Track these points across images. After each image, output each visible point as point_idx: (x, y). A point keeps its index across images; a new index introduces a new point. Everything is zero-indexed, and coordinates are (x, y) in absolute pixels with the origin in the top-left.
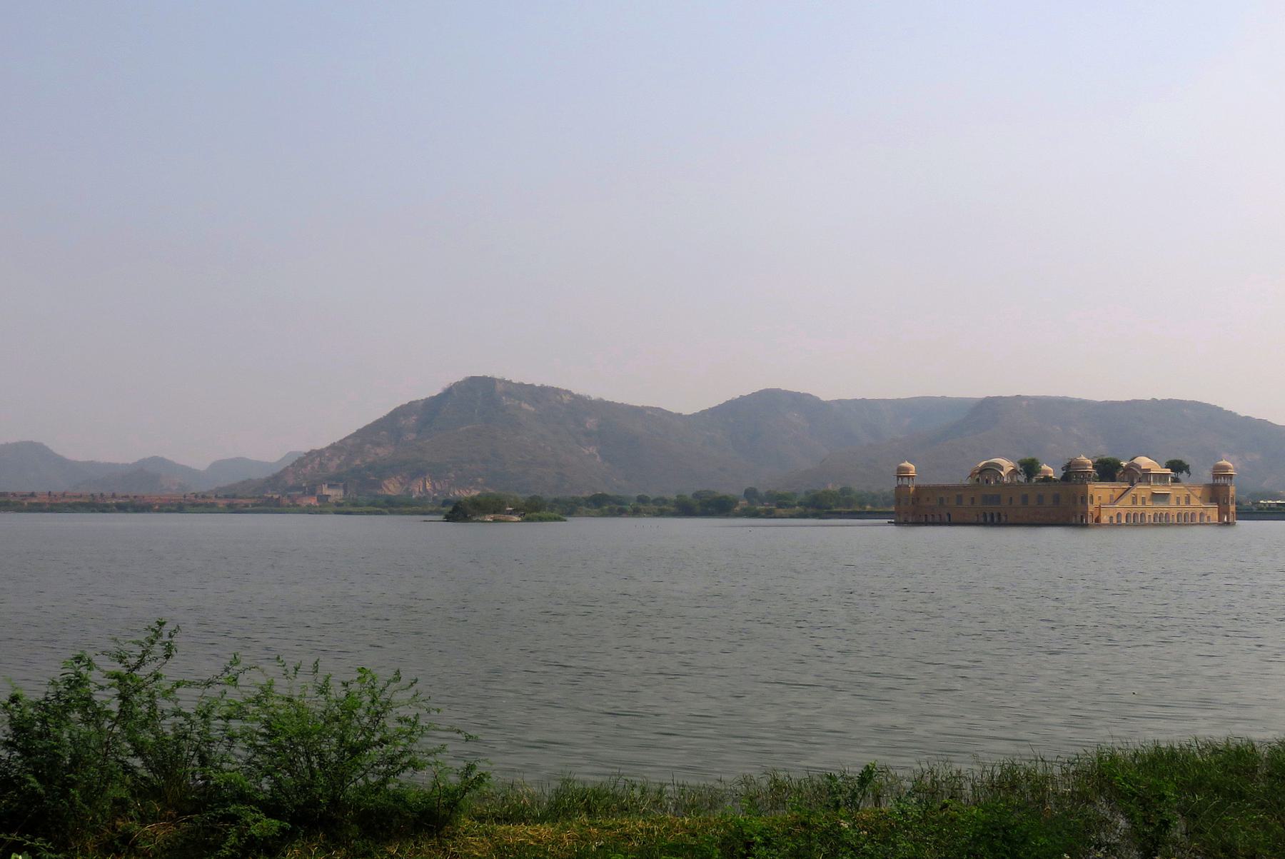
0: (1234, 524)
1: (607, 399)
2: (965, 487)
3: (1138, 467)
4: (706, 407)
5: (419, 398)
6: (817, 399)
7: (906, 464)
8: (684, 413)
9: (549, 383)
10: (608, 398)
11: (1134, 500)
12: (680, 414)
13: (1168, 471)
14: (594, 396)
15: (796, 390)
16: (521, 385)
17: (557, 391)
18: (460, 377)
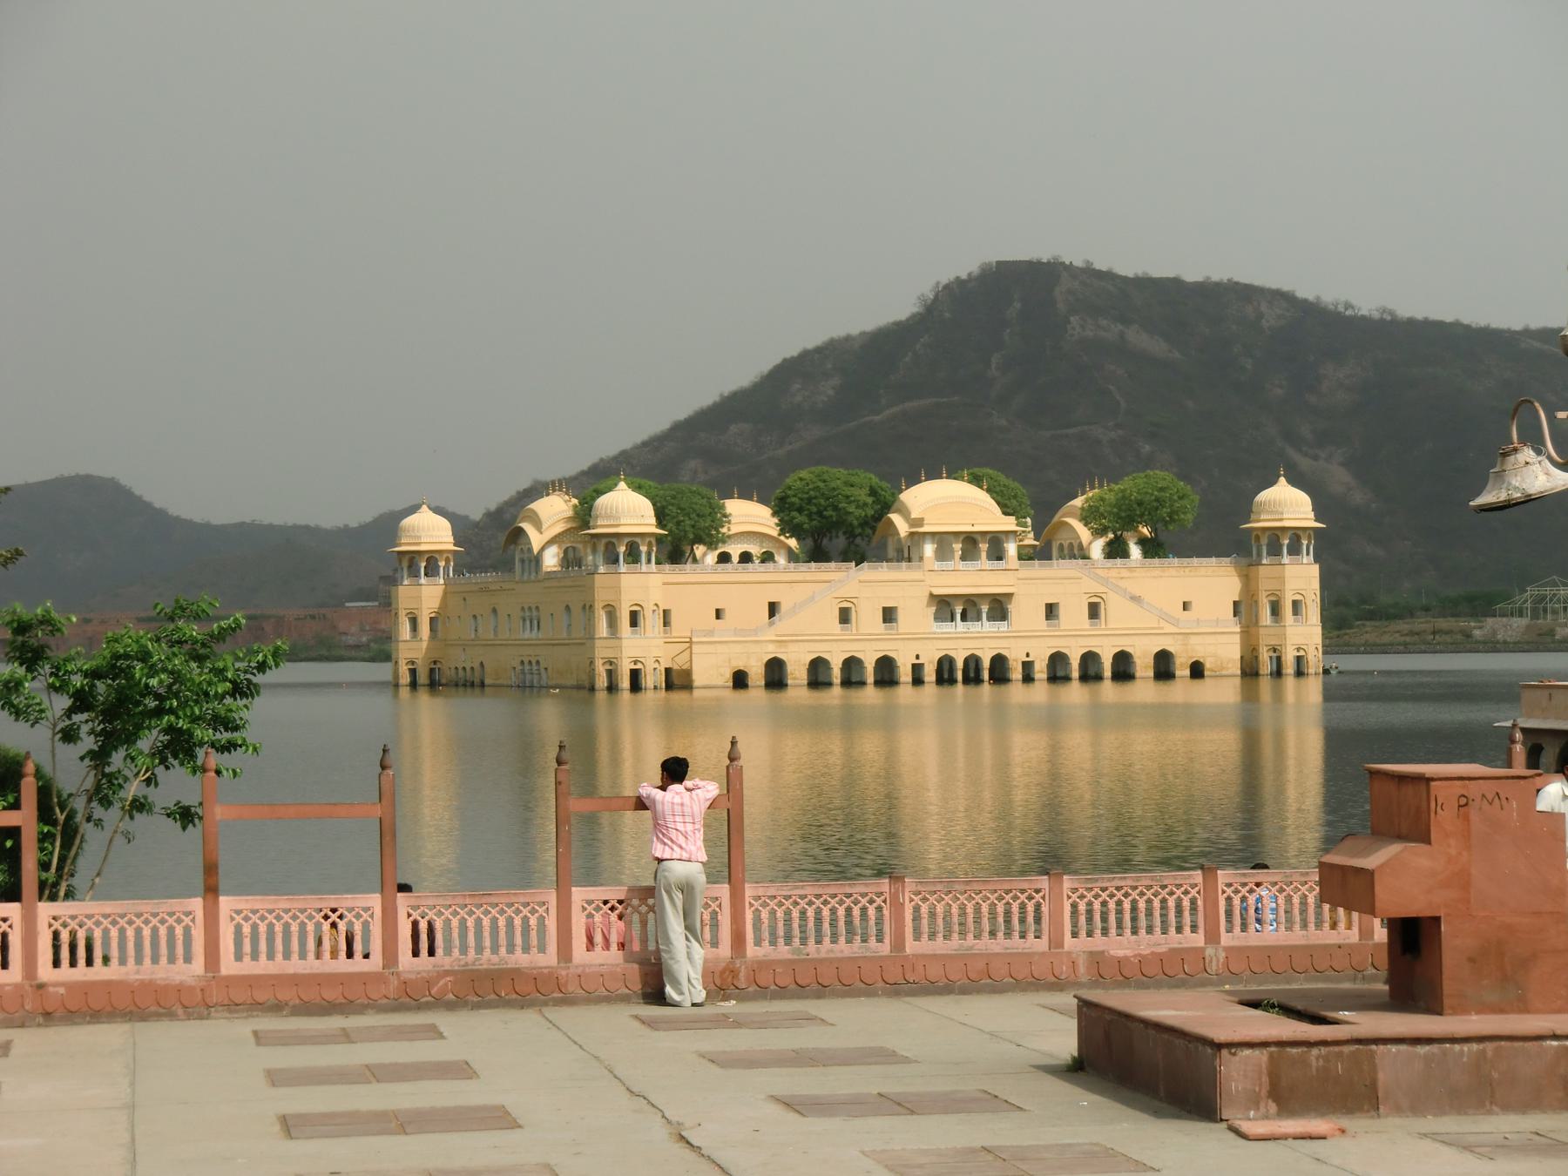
3: (905, 512)
9: (1219, 274)
11: (844, 616)
13: (1009, 524)
16: (1144, 283)
17: (1247, 293)
18: (965, 264)
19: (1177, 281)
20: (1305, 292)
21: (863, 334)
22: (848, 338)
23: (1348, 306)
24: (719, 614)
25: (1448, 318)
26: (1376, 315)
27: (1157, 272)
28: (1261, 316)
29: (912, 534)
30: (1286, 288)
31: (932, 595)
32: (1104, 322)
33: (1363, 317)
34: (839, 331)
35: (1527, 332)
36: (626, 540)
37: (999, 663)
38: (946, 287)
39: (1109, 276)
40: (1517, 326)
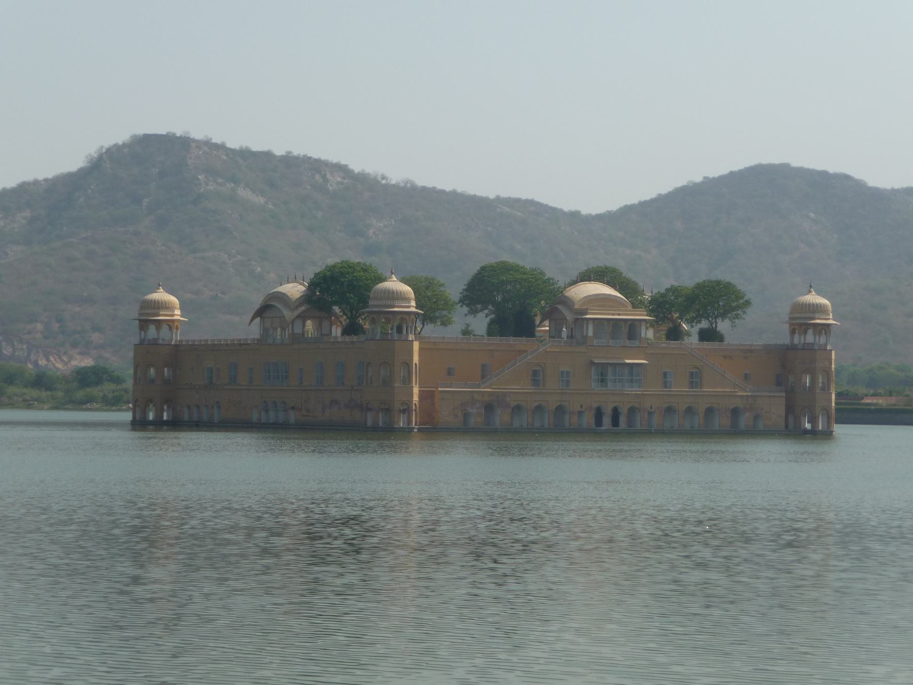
0: (827, 435)
1: (421, 182)
2: (241, 347)
4: (633, 200)
5: (41, 177)
6: (859, 187)
7: (161, 295)
8: (585, 211)
9: (299, 150)
10: (423, 180)
11: (536, 377)
12: (575, 215)
14: (396, 174)
15: (819, 166)
16: (245, 154)
17: (317, 166)
18: (120, 135)
19: (268, 155)
20: (356, 167)
21: (46, 180)
22: (36, 182)
23: (383, 178)
24: (450, 372)
25: (448, 188)
26: (402, 184)
27: (256, 147)
28: (326, 181)
29: (577, 319)
30: (343, 162)
31: (592, 363)
32: (220, 180)
33: (394, 185)
34: (29, 177)
35: (498, 199)
36: (399, 317)
37: (632, 411)
38: (109, 150)
39: (222, 147)
40: (492, 196)
